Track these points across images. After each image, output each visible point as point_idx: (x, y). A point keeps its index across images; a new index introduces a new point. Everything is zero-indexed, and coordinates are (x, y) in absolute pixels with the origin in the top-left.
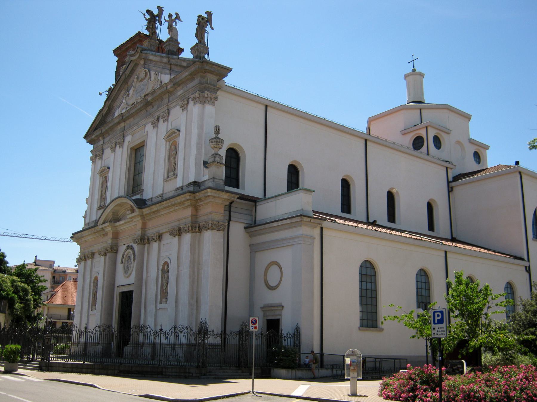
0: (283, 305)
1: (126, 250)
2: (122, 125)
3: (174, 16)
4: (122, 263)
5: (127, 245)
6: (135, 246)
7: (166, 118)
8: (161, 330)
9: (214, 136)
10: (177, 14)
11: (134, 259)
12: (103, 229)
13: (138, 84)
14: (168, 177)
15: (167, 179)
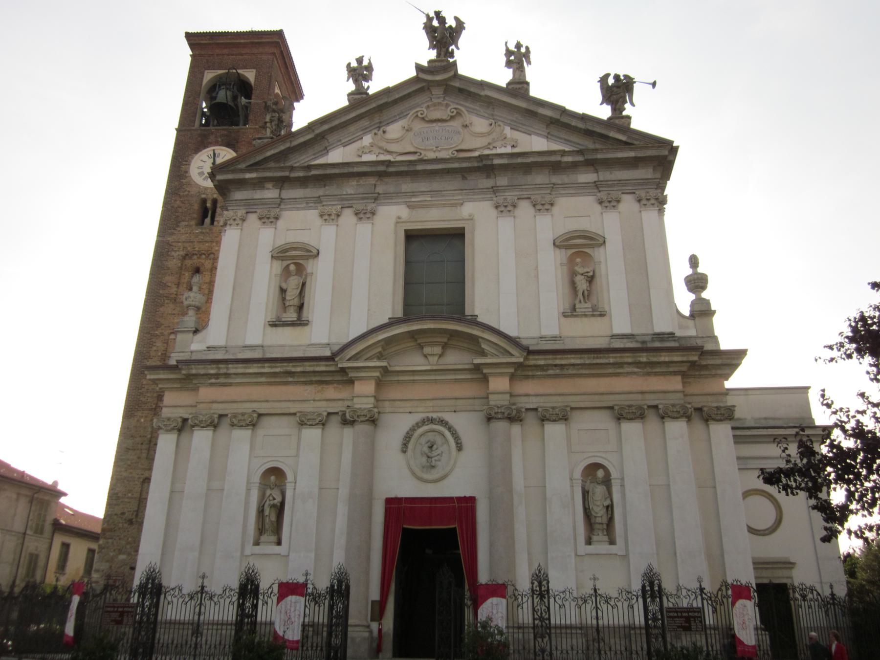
0: (792, 561)
1: (418, 425)
2: (372, 181)
3: (523, 50)
4: (404, 448)
5: (424, 415)
6: (466, 423)
7: (547, 207)
8: (833, 594)
9: (690, 271)
10: (527, 48)
11: (460, 448)
12: (343, 371)
13: (418, 126)
14: (574, 309)
15: (571, 313)
